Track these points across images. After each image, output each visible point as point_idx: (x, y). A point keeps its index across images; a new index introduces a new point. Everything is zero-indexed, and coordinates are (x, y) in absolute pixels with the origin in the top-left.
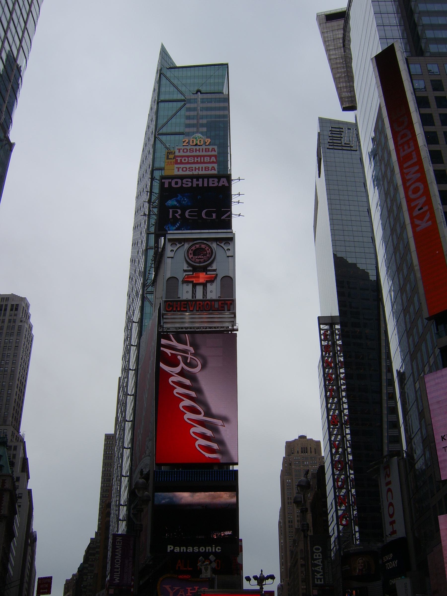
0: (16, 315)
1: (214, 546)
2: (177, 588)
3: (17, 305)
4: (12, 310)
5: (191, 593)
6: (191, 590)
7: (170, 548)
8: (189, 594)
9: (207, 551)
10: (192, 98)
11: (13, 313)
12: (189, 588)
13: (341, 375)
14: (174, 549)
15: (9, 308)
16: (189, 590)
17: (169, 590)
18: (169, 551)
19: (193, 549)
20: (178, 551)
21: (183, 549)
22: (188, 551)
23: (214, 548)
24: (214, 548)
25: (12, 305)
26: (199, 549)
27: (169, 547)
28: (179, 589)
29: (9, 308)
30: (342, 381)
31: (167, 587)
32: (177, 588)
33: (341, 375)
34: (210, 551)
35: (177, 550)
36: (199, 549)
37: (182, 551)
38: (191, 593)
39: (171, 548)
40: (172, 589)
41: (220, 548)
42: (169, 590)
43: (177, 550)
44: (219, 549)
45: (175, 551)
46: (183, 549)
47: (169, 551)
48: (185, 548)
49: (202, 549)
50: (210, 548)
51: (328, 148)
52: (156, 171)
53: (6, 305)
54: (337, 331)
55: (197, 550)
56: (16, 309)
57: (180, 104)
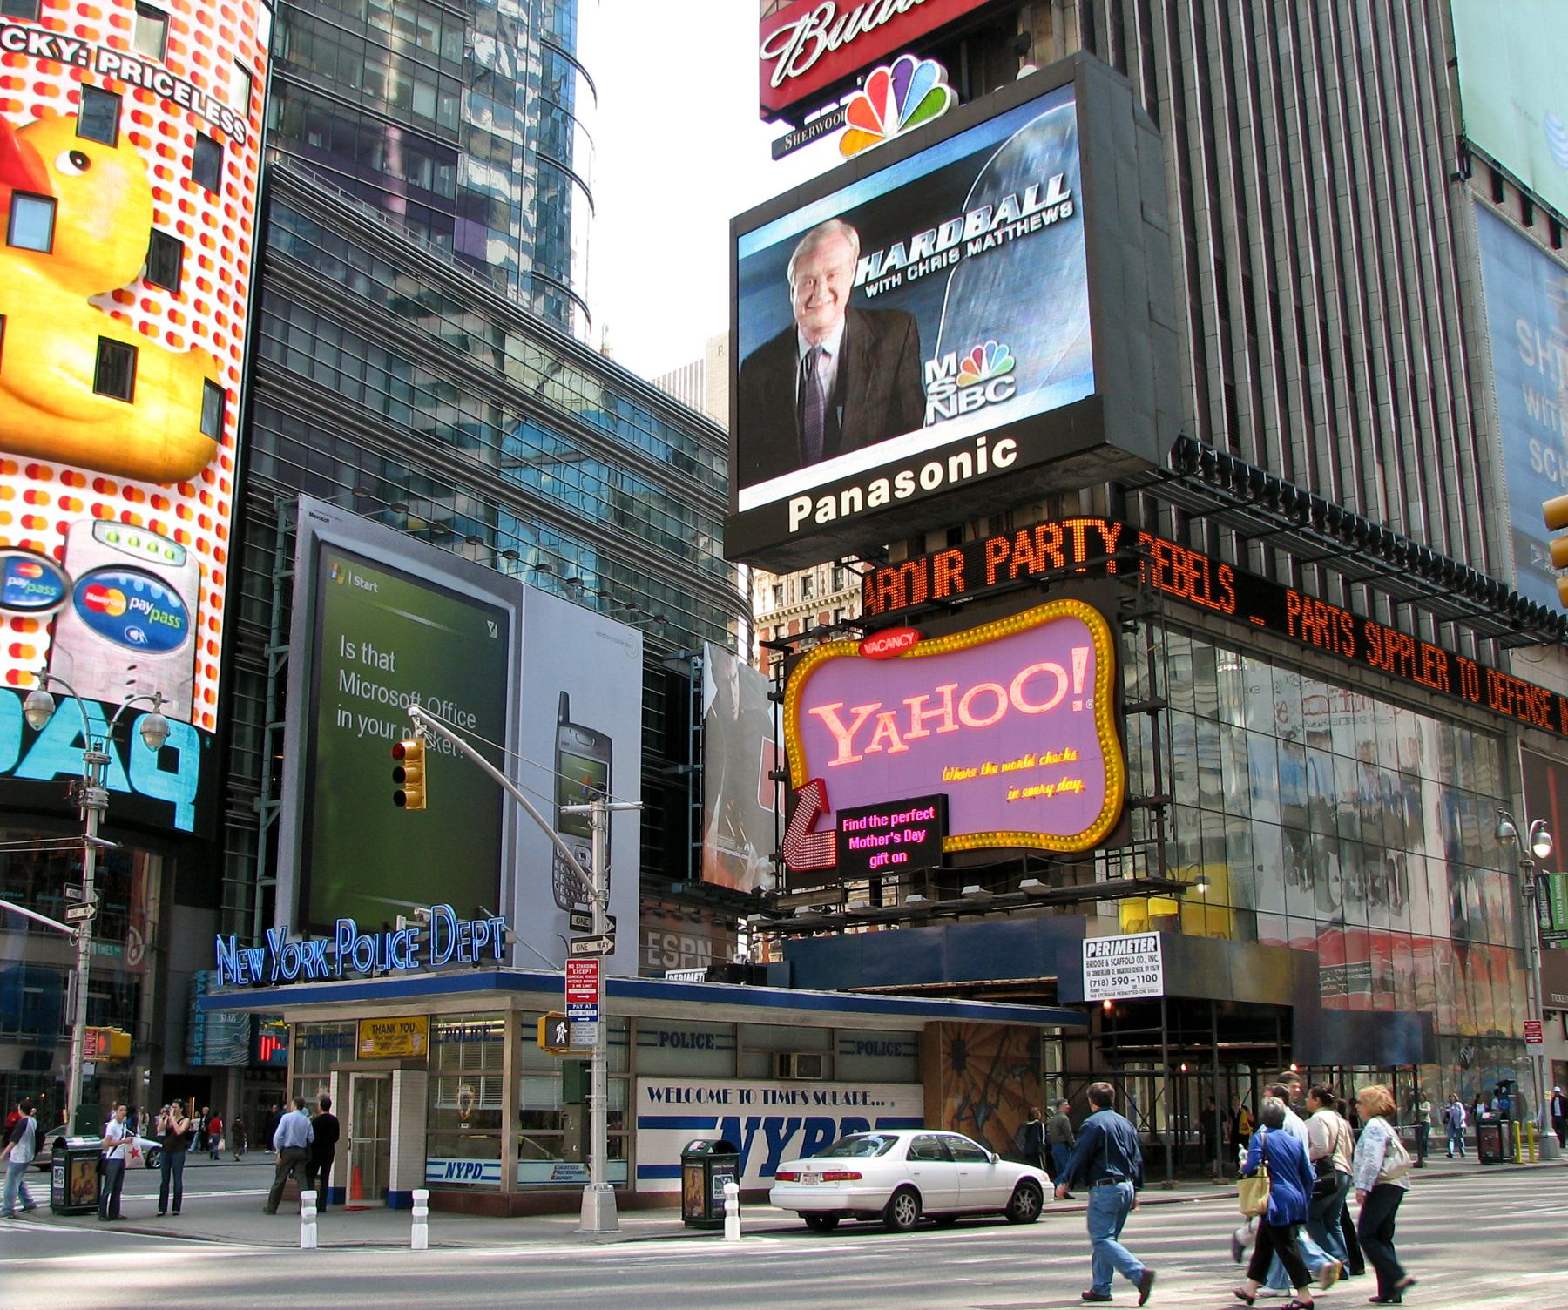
2: (864, 711)
5: (925, 723)
8: (917, 731)
12: (915, 702)
14: (814, 510)
16: (916, 710)
18: (794, 527)
19: (893, 488)
22: (873, 502)
23: (982, 454)
24: (982, 454)
28: (874, 713)
31: (827, 713)
32: (864, 711)
34: (967, 473)
36: (916, 479)
38: (925, 723)
40: (846, 719)
41: (1009, 443)
42: (835, 725)
44: (1005, 453)
45: (820, 519)
47: (794, 527)
55: (911, 487)
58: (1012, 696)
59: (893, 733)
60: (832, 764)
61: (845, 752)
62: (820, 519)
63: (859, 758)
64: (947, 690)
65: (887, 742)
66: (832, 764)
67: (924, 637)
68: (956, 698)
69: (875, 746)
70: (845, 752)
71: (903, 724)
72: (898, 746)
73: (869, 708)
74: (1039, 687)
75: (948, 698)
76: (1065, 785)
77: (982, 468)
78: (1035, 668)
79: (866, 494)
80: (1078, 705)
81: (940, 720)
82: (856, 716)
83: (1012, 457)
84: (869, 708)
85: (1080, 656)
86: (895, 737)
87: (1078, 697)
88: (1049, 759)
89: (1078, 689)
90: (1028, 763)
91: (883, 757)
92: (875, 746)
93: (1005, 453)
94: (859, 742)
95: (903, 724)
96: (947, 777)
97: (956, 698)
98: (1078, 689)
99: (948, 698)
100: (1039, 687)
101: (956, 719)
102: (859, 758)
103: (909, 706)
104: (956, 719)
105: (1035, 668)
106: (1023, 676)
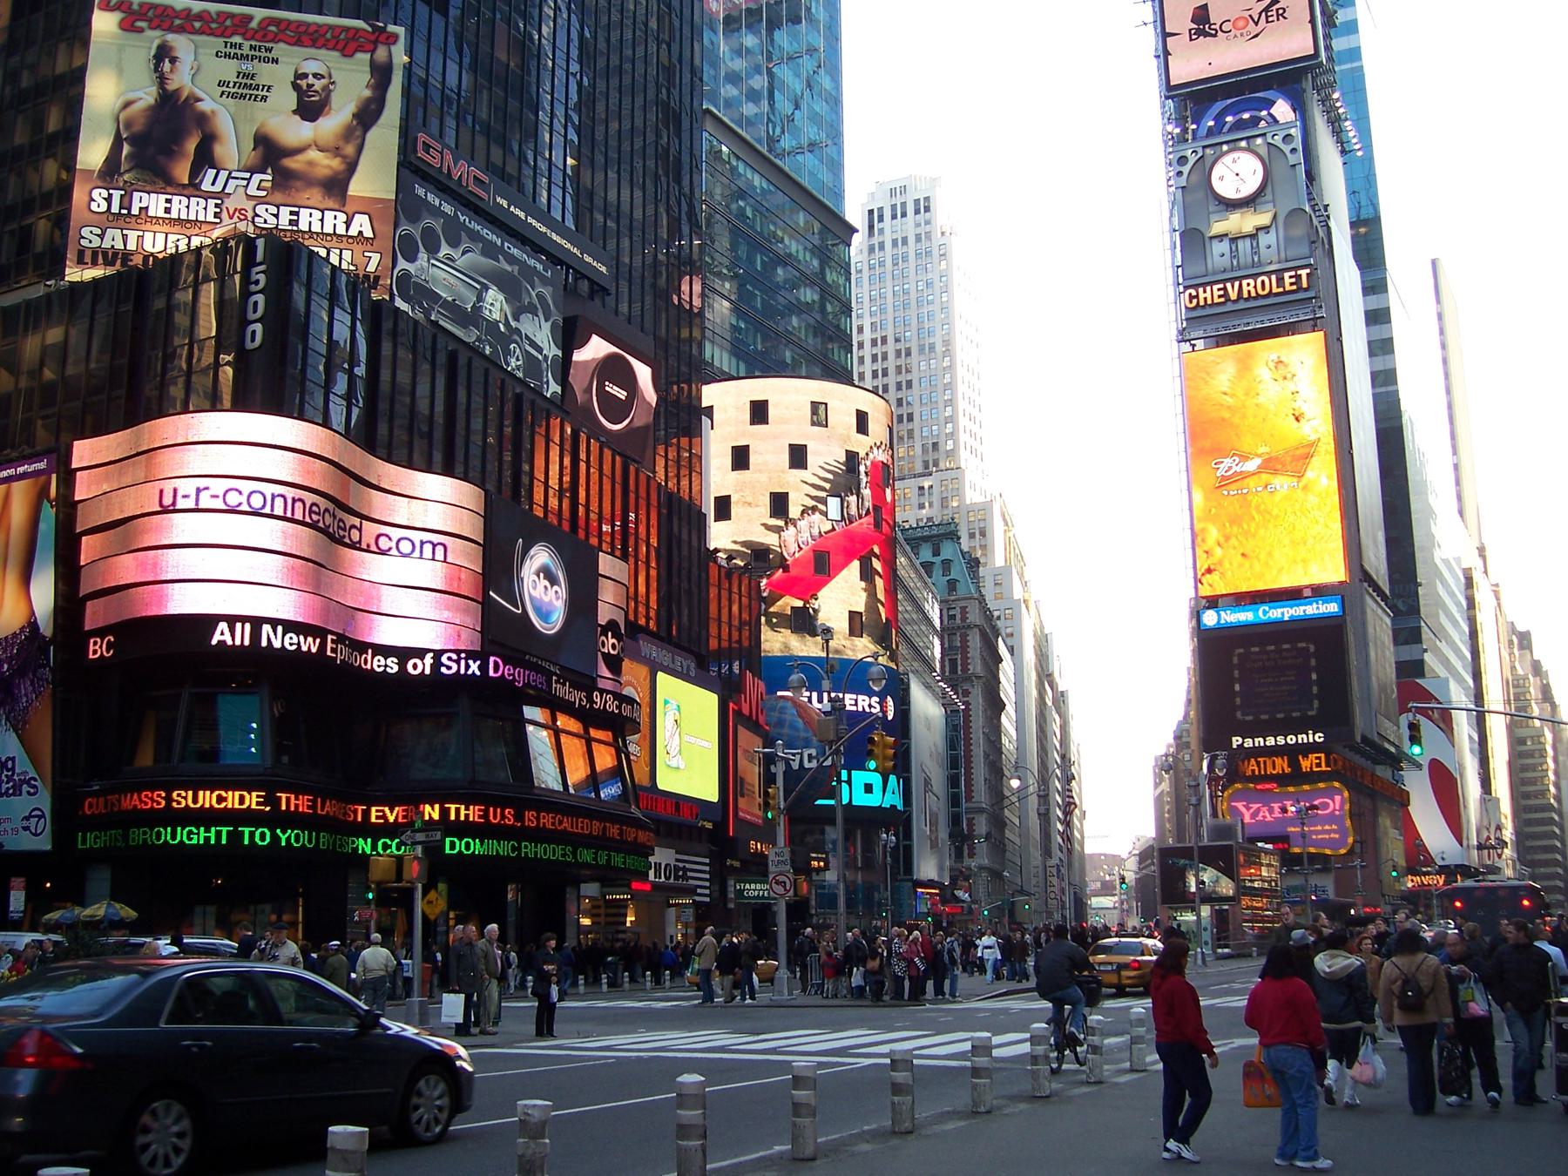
0: (928, 223)
3: (927, 199)
4: (917, 212)
7: (1236, 741)
11: (921, 217)
15: (910, 209)
17: (1243, 810)
25: (917, 202)
29: (910, 209)
31: (1240, 805)
32: (1256, 806)
35: (1248, 743)
40: (1248, 809)
42: (1243, 810)
43: (1248, 743)
53: (904, 204)
56: (927, 209)
69: (1260, 818)
71: (1271, 811)
72: (1269, 818)
91: (1263, 822)
92: (1260, 818)
94: (1253, 816)
95: (1271, 811)
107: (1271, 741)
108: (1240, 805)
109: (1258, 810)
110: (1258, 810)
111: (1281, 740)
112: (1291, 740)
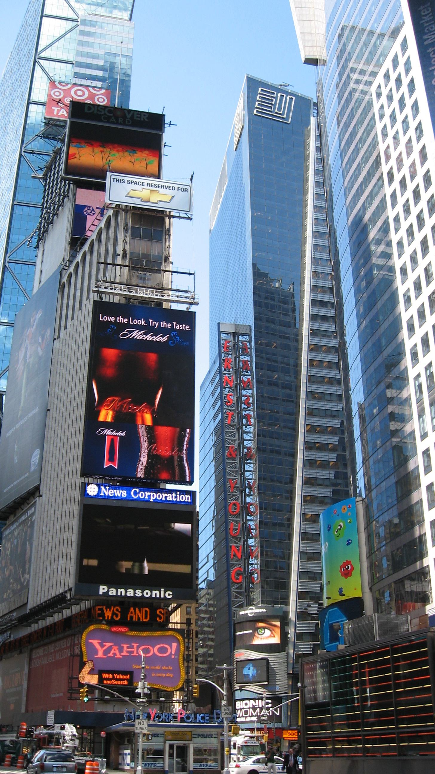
1: (162, 590)
2: (108, 645)
5: (128, 652)
6: (128, 647)
7: (103, 589)
8: (125, 653)
9: (154, 596)
10: (87, 19)
12: (125, 646)
13: (243, 398)
14: (108, 591)
16: (125, 648)
18: (101, 593)
19: (135, 593)
20: (114, 594)
21: (121, 592)
22: (128, 594)
23: (162, 593)
24: (162, 593)
26: (142, 593)
27: (101, 587)
28: (111, 646)
30: (243, 405)
31: (95, 643)
32: (108, 645)
33: (243, 398)
35: (113, 592)
37: (119, 594)
38: (128, 652)
39: (104, 589)
40: (102, 646)
41: (171, 593)
42: (98, 646)
43: (113, 592)
45: (110, 593)
46: (121, 592)
47: (101, 593)
48: (123, 591)
49: (147, 594)
50: (158, 592)
51: (255, 115)
52: (33, 105)
54: (241, 344)
57: (71, 24)
58: (155, 650)
59: (117, 652)
60: (96, 656)
61: (100, 654)
62: (110, 593)
63: (105, 657)
64: (135, 645)
65: (115, 654)
66: (96, 656)
67: (131, 630)
68: (138, 647)
69: (111, 654)
70: (100, 654)
71: (121, 650)
72: (118, 656)
73: (110, 644)
74: (162, 650)
75: (135, 647)
76: (168, 675)
77: (162, 596)
78: (162, 645)
79: (126, 592)
80: (173, 657)
81: (133, 652)
82: (105, 645)
83: (171, 597)
84: (110, 644)
85: (175, 645)
86: (118, 653)
87: (173, 655)
88: (164, 668)
89: (173, 653)
90: (158, 667)
92: (111, 654)
93: (169, 595)
94: (106, 652)
95: (121, 650)
96: (134, 667)
97: (138, 647)
98: (173, 653)
99: (135, 647)
100: (162, 650)
101: (137, 653)
102: (105, 657)
103: (123, 647)
104: (137, 653)
105: (162, 645)
106: (158, 646)
107: (130, 593)
108: (95, 643)
109: (110, 648)
110: (110, 648)
111: (139, 593)
112: (147, 594)
